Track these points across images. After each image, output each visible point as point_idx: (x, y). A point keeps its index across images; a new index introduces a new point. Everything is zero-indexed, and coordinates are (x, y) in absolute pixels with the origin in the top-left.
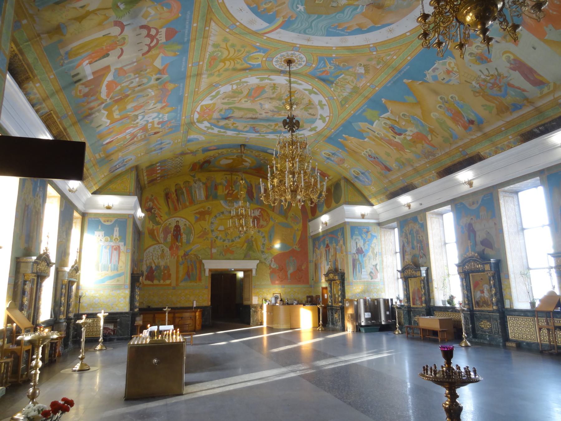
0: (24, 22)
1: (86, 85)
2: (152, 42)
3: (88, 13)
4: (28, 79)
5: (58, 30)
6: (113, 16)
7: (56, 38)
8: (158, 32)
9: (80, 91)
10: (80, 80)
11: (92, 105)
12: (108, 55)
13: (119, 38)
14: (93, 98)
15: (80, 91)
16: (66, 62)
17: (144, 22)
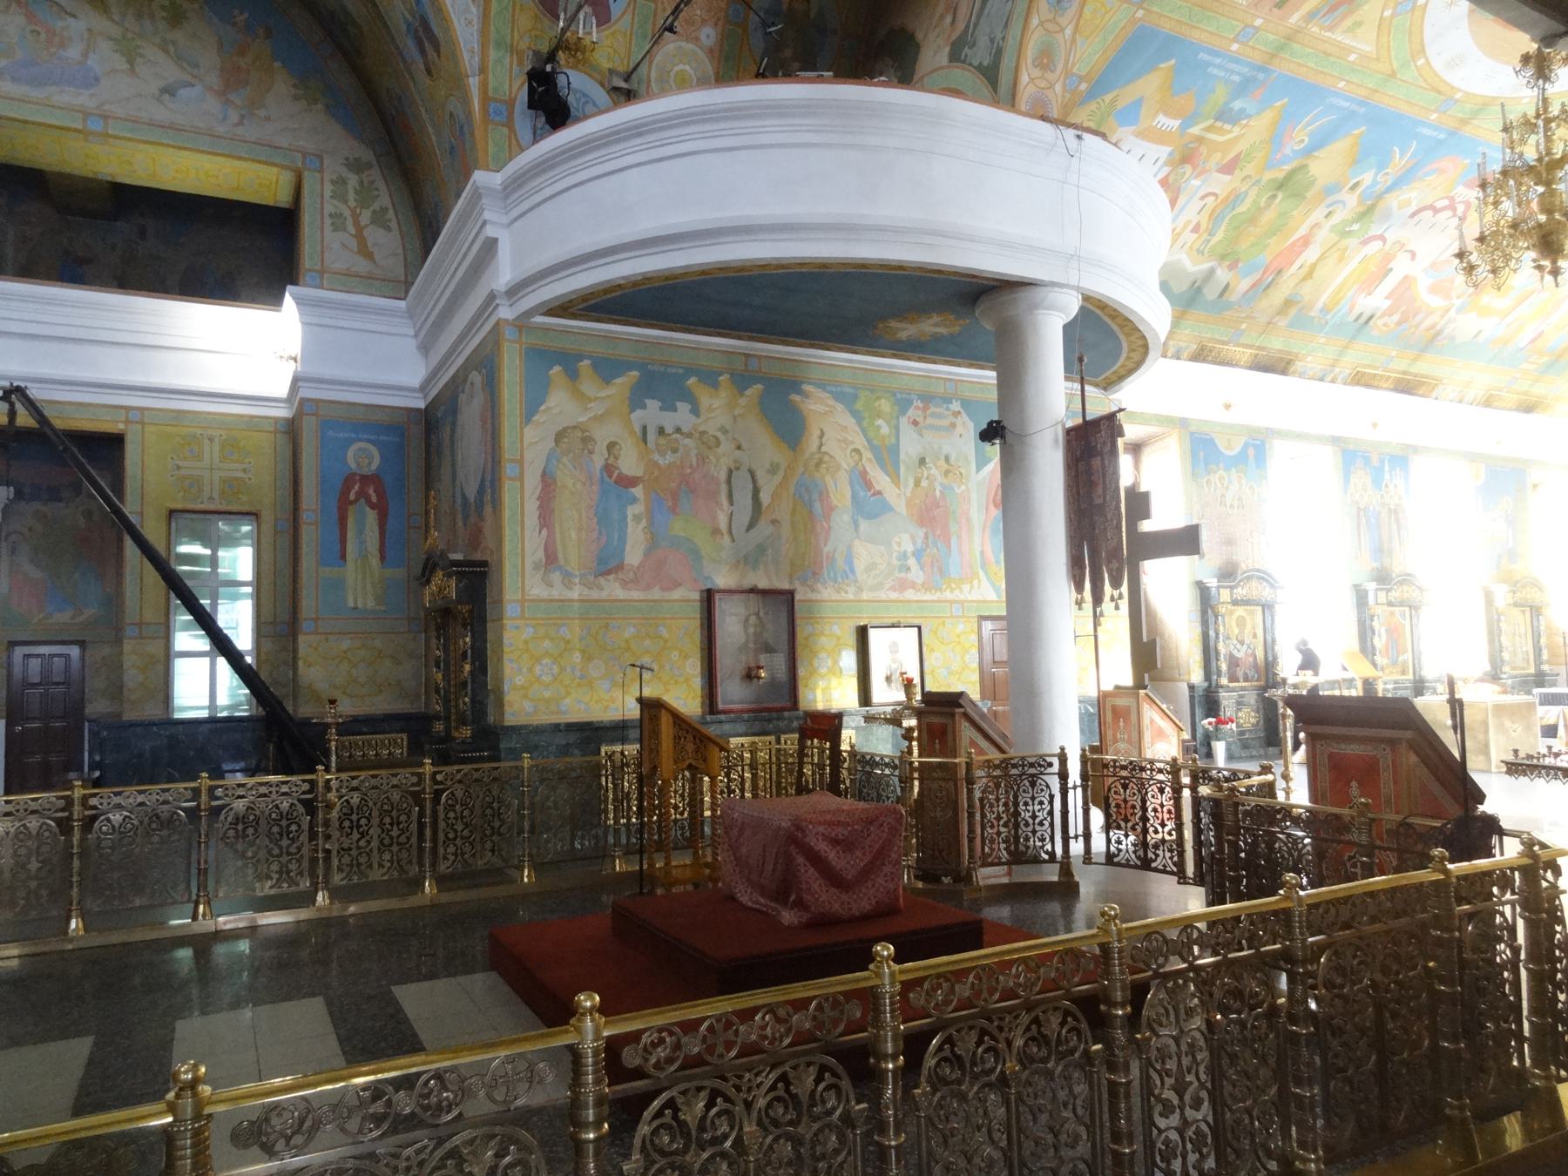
0: (1244, 326)
1: (1389, 312)
2: (1454, 209)
3: (1313, 267)
4: (1289, 362)
5: (1288, 303)
6: (1352, 242)
7: (1293, 311)
8: (1452, 199)
9: (1385, 325)
10: (1371, 317)
11: (1427, 323)
12: (1391, 270)
13: (1388, 247)
14: (1418, 318)
15: (1385, 325)
16: (1328, 317)
17: (1413, 208)
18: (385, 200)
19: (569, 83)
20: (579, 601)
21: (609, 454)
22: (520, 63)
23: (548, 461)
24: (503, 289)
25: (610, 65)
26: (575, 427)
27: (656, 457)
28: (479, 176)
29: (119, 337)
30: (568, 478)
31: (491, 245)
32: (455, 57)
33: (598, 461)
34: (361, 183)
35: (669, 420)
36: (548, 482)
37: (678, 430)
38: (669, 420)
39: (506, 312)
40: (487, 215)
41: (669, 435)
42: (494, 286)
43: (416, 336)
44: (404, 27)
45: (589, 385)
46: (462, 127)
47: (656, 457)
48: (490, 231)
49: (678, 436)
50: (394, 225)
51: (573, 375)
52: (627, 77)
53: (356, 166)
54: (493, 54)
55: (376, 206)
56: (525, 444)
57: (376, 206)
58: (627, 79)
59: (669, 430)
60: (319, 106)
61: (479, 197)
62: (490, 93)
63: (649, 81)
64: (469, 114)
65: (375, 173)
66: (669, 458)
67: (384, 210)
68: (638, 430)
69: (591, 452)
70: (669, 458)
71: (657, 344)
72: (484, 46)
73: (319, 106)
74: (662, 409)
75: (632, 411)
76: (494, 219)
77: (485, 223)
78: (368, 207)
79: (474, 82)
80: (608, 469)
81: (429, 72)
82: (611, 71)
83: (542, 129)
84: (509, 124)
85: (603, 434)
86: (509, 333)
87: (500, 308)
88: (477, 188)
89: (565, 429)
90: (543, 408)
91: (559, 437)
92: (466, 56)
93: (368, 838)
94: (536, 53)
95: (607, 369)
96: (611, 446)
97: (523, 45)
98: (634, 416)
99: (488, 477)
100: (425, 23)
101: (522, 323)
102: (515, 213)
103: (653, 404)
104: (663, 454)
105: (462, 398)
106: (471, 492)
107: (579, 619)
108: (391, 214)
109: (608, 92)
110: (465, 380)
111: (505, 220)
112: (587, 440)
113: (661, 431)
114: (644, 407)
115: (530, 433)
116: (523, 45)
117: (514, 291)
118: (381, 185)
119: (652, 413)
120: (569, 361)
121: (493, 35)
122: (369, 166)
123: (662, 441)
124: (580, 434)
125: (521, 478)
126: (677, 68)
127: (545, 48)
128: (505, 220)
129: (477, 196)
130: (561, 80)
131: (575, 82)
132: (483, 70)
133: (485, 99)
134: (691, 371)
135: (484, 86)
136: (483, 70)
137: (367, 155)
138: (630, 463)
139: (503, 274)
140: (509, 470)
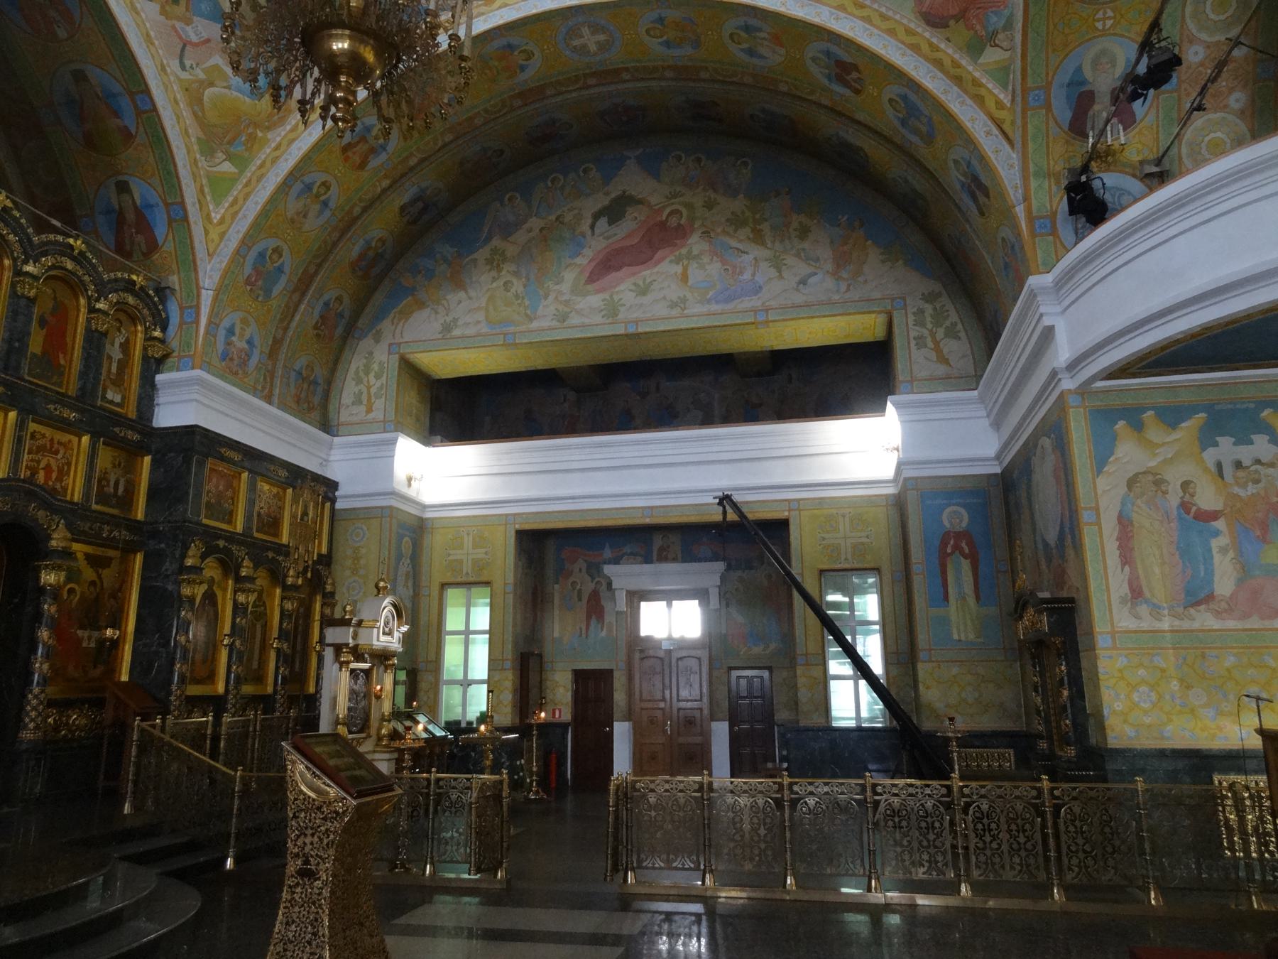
18: (954, 317)
19: (1104, 184)
20: (1172, 631)
21: (1184, 492)
22: (1058, 183)
23: (1123, 504)
24: (1064, 365)
25: (1140, 158)
26: (1144, 473)
27: (1236, 490)
28: (1033, 281)
29: (801, 452)
30: (1143, 518)
31: (1050, 331)
32: (1002, 195)
33: (1174, 500)
34: (935, 309)
35: (1245, 453)
36: (1125, 525)
37: (1258, 462)
38: (1245, 453)
39: (1068, 384)
40: (1042, 309)
41: (1248, 467)
42: (1056, 365)
43: (988, 416)
44: (958, 187)
45: (1155, 432)
46: (1013, 247)
47: (1236, 490)
48: (1047, 321)
49: (1258, 467)
50: (962, 334)
51: (1138, 426)
52: (1159, 162)
53: (929, 298)
54: (1033, 184)
55: (948, 323)
56: (1099, 492)
57: (948, 323)
58: (1157, 165)
59: (1246, 463)
60: (901, 262)
61: (1035, 296)
62: (1035, 214)
63: (1180, 158)
64: (1019, 235)
65: (945, 300)
66: (1251, 489)
67: (954, 325)
68: (1213, 469)
69: (1165, 493)
70: (1251, 489)
71: (1221, 385)
72: (1025, 178)
73: (901, 262)
74: (1235, 444)
75: (1204, 449)
76: (1050, 313)
77: (1041, 315)
78: (941, 326)
79: (1020, 211)
80: (1185, 506)
81: (982, 214)
82: (1142, 163)
83: (1082, 228)
84: (1054, 232)
85: (1174, 477)
86: (1072, 401)
87: (1063, 381)
88: (1032, 290)
89: (1136, 475)
90: (1111, 459)
91: (1131, 483)
92: (1011, 192)
93: (1033, 842)
94: (1070, 170)
95: (1172, 416)
96: (1185, 485)
97: (1058, 168)
98: (1206, 455)
99: (1067, 525)
100: (975, 179)
101: (1084, 390)
102: (1067, 302)
103: (1225, 442)
104: (1244, 486)
105: (1035, 461)
106: (1052, 537)
107: (1174, 649)
108: (960, 326)
109: (1141, 180)
110: (1036, 446)
111: (1059, 309)
112: (1159, 482)
113: (1238, 465)
114: (1216, 444)
115: (1102, 483)
116: (1058, 168)
117: (1073, 366)
118: (950, 307)
119: (1226, 448)
120: (1133, 416)
121: (1032, 168)
122: (940, 294)
123: (1241, 474)
124: (1151, 478)
125: (1098, 523)
126: (1207, 139)
127: (1078, 163)
128: (1059, 309)
129: (1033, 295)
130: (1096, 184)
131: (1108, 181)
132: (1026, 199)
133: (1031, 219)
134: (1264, 404)
135: (1029, 210)
136: (1026, 199)
137: (936, 286)
138: (1207, 498)
139: (1063, 352)
140: (1086, 516)
